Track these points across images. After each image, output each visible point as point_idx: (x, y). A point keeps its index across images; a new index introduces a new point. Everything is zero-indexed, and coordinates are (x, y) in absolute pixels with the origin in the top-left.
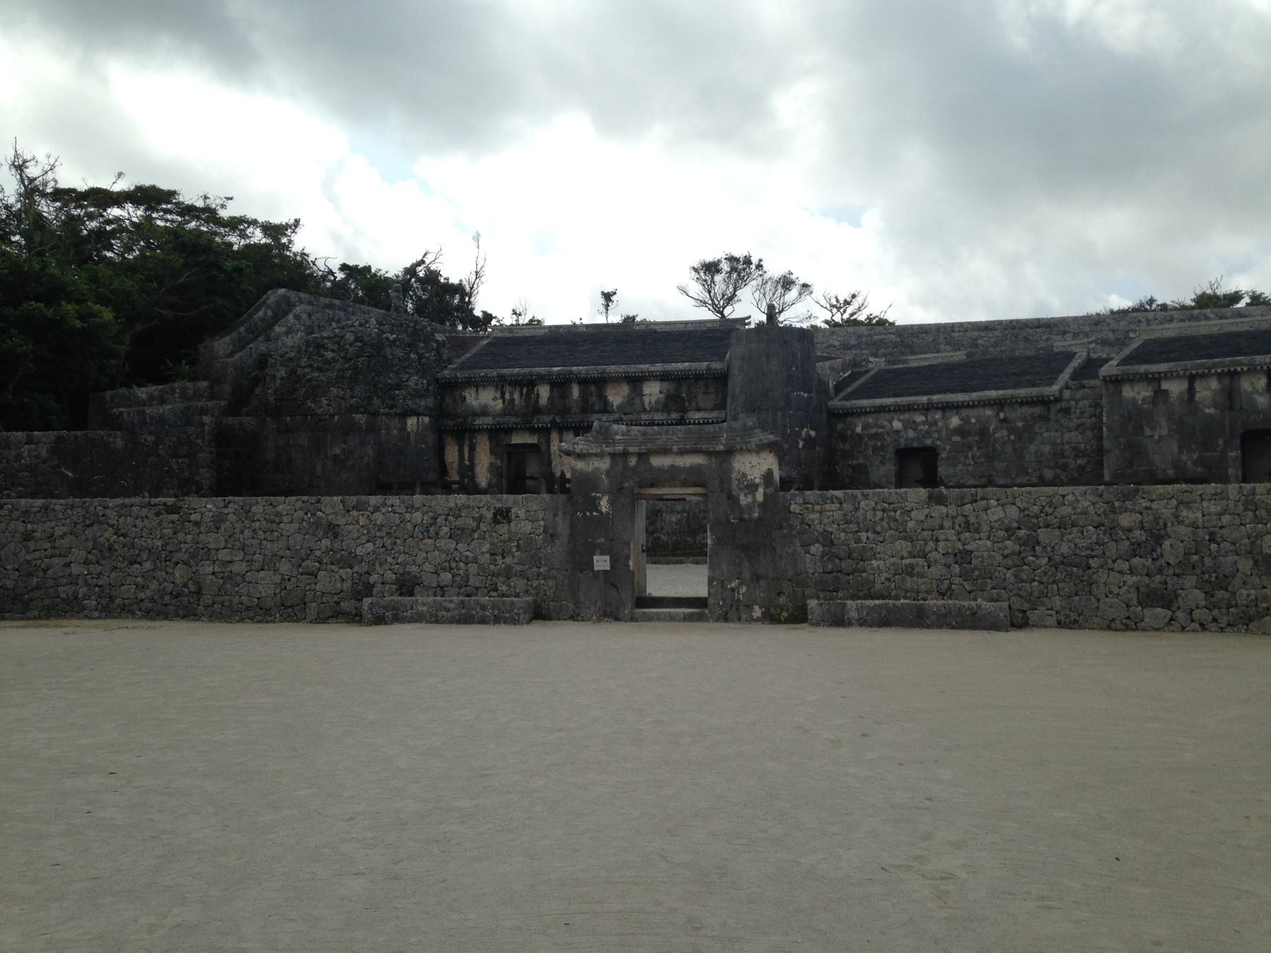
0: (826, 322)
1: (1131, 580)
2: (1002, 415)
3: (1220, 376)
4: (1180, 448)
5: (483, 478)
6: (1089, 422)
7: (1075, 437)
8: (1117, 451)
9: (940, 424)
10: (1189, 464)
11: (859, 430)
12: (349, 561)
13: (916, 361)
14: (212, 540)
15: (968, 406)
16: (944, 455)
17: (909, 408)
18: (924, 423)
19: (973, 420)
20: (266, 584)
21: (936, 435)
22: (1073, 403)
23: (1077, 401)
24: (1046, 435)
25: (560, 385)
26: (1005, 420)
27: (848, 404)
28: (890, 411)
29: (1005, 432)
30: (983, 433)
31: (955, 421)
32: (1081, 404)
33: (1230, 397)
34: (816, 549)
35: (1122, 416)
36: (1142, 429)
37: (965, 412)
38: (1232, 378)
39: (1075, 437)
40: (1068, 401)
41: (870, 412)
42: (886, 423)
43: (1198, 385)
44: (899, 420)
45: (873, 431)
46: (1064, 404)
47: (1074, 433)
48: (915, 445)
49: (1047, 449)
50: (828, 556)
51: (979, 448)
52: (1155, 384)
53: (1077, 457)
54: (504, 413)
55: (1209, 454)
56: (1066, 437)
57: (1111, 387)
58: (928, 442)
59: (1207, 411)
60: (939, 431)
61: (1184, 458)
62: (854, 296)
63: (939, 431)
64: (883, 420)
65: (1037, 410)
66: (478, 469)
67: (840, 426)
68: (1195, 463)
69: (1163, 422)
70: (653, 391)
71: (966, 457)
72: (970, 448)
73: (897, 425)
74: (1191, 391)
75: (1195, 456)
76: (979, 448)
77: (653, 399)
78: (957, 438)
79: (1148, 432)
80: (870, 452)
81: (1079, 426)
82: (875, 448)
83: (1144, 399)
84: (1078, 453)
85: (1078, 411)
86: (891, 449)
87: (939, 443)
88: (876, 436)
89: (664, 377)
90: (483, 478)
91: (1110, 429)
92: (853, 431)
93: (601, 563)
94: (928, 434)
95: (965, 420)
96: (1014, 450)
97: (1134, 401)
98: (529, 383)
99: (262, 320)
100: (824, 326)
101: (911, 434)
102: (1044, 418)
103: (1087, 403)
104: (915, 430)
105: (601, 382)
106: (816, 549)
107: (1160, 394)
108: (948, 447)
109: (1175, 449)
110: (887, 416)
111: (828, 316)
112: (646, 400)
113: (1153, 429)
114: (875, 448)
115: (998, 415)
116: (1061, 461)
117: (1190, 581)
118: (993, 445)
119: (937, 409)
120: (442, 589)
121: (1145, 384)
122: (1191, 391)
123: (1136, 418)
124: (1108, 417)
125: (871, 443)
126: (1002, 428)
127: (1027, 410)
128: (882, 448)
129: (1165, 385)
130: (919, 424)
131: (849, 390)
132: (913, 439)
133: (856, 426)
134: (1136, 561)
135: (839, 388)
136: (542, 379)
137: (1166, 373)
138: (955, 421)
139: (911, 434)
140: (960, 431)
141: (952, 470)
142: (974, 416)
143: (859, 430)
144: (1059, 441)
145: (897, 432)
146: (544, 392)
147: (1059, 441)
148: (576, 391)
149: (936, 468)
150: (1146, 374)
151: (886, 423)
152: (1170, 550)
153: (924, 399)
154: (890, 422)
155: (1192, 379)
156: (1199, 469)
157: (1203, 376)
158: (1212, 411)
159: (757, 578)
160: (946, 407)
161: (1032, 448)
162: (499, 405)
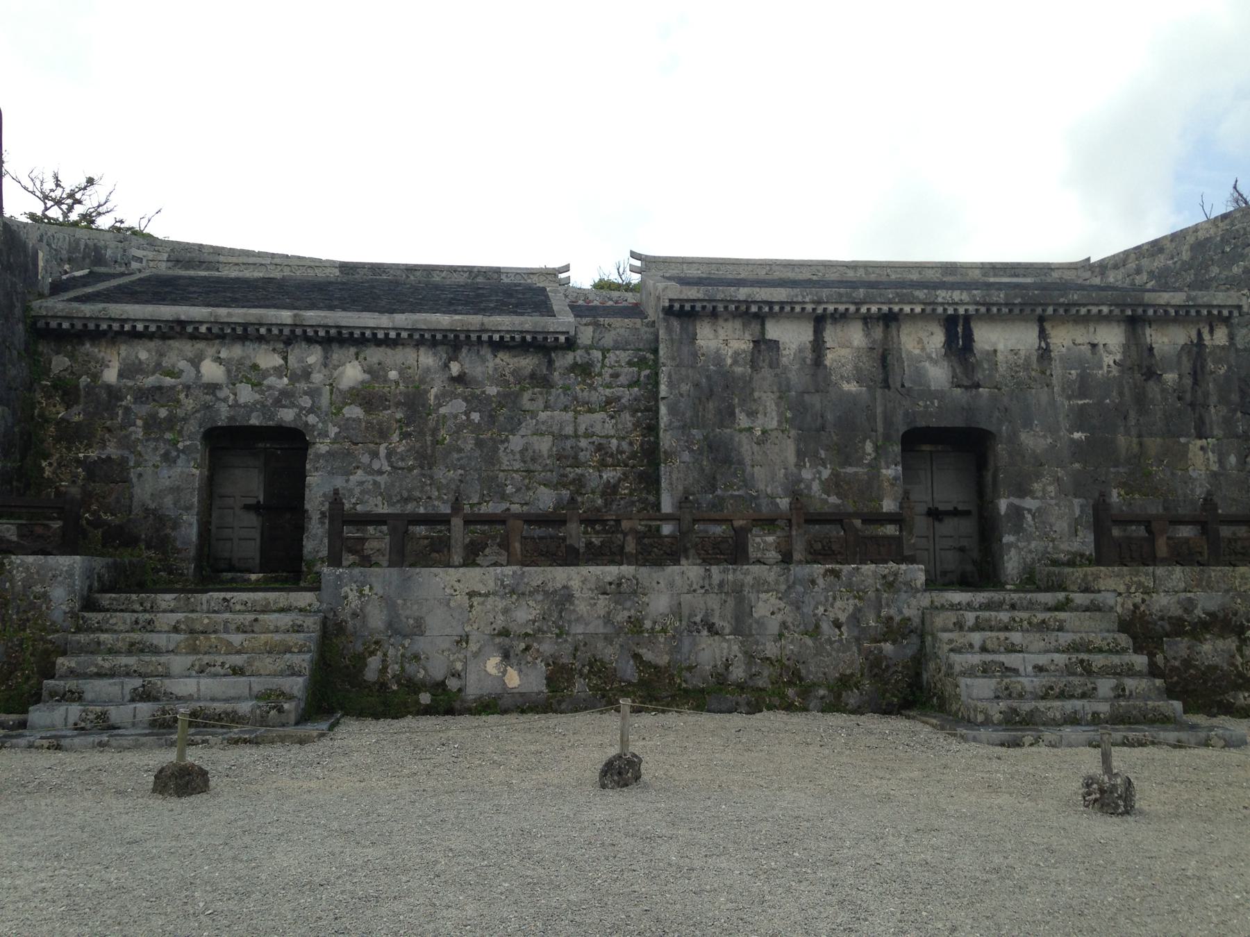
0: (32, 216)
2: (455, 368)
3: (867, 320)
4: (800, 454)
6: (627, 395)
7: (599, 422)
8: (686, 456)
9: (317, 378)
10: (816, 486)
15: (378, 343)
16: (322, 447)
18: (279, 372)
19: (393, 375)
21: (306, 402)
22: (597, 354)
23: (605, 351)
24: (543, 416)
26: (460, 379)
27: (88, 309)
28: (195, 337)
29: (459, 406)
30: (415, 403)
31: (352, 373)
32: (611, 357)
33: (884, 360)
35: (697, 385)
36: (733, 414)
37: (375, 355)
38: (887, 326)
39: (599, 422)
40: (588, 349)
41: (150, 336)
42: (182, 364)
43: (831, 335)
44: (218, 360)
45: (150, 381)
46: (578, 356)
47: (600, 416)
48: (254, 421)
49: (544, 445)
51: (406, 435)
52: (755, 327)
53: (603, 465)
55: (850, 470)
56: (585, 420)
57: (676, 324)
58: (287, 416)
59: (845, 387)
60: (314, 393)
61: (807, 474)
62: (91, 181)
63: (314, 393)
64: (178, 354)
65: (527, 363)
67: (60, 363)
68: (827, 487)
69: (769, 400)
71: (375, 455)
72: (384, 434)
73: (211, 371)
74: (818, 346)
75: (826, 473)
76: (406, 435)
78: (353, 412)
79: (743, 420)
80: (138, 432)
81: (609, 402)
82: (152, 423)
83: (737, 353)
84: (605, 457)
85: (607, 372)
86: (193, 427)
87: (312, 419)
91: (673, 410)
92: (96, 376)
94: (285, 397)
95: (376, 373)
96: (479, 443)
97: (718, 359)
100: (24, 219)
101: (246, 394)
102: (541, 381)
103: (624, 356)
104: (256, 385)
107: (764, 347)
108: (333, 431)
109: (792, 458)
110: (189, 348)
111: (38, 208)
113: (752, 414)
114: (152, 423)
115: (446, 366)
116: (572, 473)
118: (435, 431)
119: (310, 341)
121: (738, 324)
122: (818, 346)
123: (721, 393)
124: (671, 385)
125: (144, 410)
126: (454, 396)
127: (507, 362)
128: (171, 422)
129: (773, 331)
130: (265, 374)
131: (89, 290)
132: (250, 408)
133: (104, 365)
135: (58, 288)
137: (782, 304)
138: (352, 373)
139: (246, 394)
140: (366, 397)
142: (396, 362)
143: (110, 375)
144: (569, 430)
145: (213, 388)
147: (569, 430)
149: (303, 476)
150: (748, 303)
151: (182, 364)
153: (286, 316)
154: (196, 362)
155: (820, 321)
156: (833, 499)
157: (841, 318)
158: (851, 387)
161: (516, 443)
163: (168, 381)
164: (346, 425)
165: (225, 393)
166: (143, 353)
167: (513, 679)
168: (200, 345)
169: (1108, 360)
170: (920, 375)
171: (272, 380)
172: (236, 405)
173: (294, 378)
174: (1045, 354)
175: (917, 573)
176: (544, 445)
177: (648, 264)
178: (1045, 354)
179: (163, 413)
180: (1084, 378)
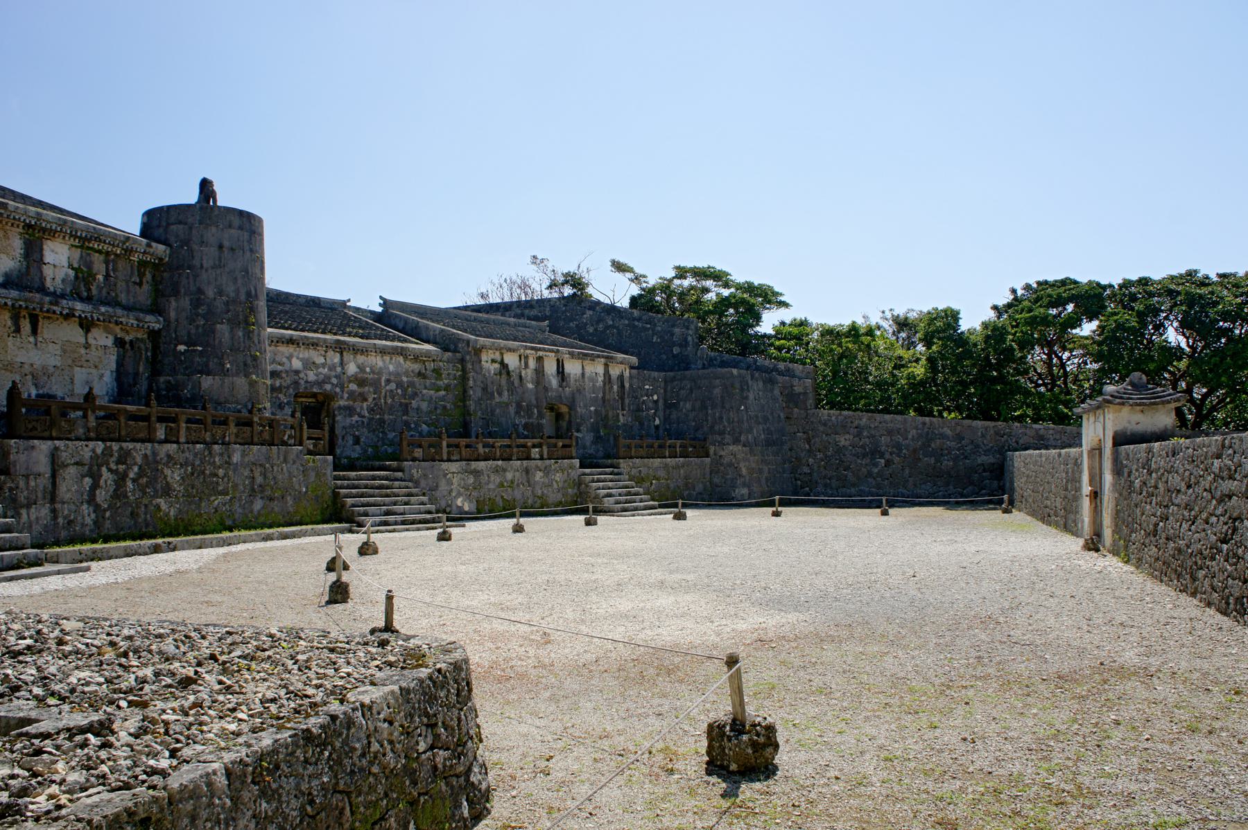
17: (315, 344)
18: (323, 365)
37: (361, 359)
42: (284, 360)
58: (328, 387)
71: (362, 408)
73: (296, 364)
77: (60, 275)
78: (353, 387)
87: (338, 390)
94: (327, 379)
95: (361, 368)
101: (311, 376)
112: (48, 271)
138: (352, 369)
141: (348, 420)
145: (297, 372)
151: (284, 360)
154: (290, 358)
163: (280, 368)
164: (351, 393)
165: (302, 375)
167: (466, 508)
168: (291, 349)
170: (550, 382)
171: (321, 370)
172: (307, 382)
173: (330, 369)
174: (583, 374)
175: (577, 462)
176: (424, 406)
177: (386, 303)
178: (583, 374)
179: (278, 384)
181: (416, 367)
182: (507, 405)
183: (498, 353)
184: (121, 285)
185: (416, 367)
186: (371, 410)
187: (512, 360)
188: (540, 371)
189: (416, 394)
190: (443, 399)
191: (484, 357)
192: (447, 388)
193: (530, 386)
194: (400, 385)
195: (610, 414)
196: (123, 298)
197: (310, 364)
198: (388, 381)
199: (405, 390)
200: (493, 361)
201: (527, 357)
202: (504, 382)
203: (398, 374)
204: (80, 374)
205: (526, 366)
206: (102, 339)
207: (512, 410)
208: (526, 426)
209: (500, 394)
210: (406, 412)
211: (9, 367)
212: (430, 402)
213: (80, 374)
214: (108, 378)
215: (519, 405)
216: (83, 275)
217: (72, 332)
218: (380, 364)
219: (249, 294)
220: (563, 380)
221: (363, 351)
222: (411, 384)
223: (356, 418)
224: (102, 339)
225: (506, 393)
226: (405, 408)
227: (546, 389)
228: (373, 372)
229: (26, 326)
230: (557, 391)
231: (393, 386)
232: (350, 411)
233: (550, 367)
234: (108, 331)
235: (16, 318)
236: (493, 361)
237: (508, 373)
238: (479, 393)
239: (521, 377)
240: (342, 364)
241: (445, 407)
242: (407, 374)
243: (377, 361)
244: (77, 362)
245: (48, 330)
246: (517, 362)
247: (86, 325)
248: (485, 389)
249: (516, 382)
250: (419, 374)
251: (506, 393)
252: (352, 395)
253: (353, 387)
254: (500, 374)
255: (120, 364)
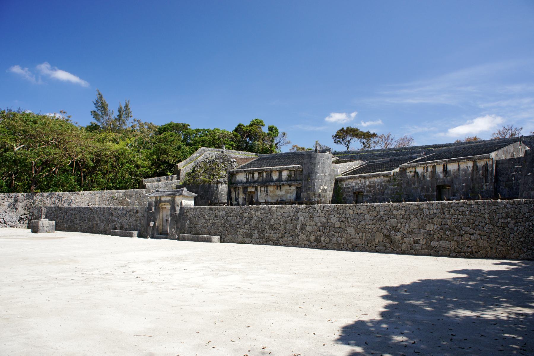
1: (245, 231)
5: (241, 201)
11: (344, 186)
12: (113, 221)
13: (376, 161)
14: (96, 216)
20: (102, 226)
25: (260, 173)
34: (188, 222)
37: (370, 179)
49: (389, 192)
50: (190, 223)
54: (247, 182)
58: (361, 189)
66: (239, 199)
70: (285, 174)
73: (354, 184)
78: (368, 188)
88: (349, 188)
89: (287, 169)
90: (241, 201)
93: (152, 224)
95: (370, 182)
98: (253, 173)
99: (196, 157)
101: (357, 187)
105: (271, 171)
106: (188, 222)
112: (283, 177)
117: (256, 231)
120: (126, 229)
134: (246, 226)
136: (255, 171)
138: (367, 183)
146: (256, 175)
148: (265, 174)
152: (253, 223)
158: (428, 179)
159: (177, 228)
160: (365, 178)
162: (245, 180)
164: (367, 190)
166: (347, 182)
169: (470, 169)
170: (439, 176)
176: (389, 192)
178: (459, 169)
180: (465, 173)
181: (387, 179)
182: (417, 188)
183: (414, 168)
184: (298, 176)
185: (387, 179)
186: (373, 195)
187: (420, 170)
188: (434, 172)
189: (386, 188)
190: (396, 189)
191: (408, 171)
192: (398, 185)
193: (428, 179)
194: (382, 186)
195: (477, 186)
196: (298, 178)
197: (357, 184)
198: (378, 185)
199: (383, 188)
200: (411, 172)
201: (427, 167)
202: (416, 179)
203: (381, 183)
204: (288, 195)
205: (427, 171)
206: (293, 188)
207: (419, 190)
208: (425, 196)
209: (414, 184)
210: (383, 195)
211: (276, 195)
212: (391, 190)
213: (288, 195)
214: (294, 195)
215: (423, 188)
216: (289, 176)
217: (287, 188)
218: (376, 180)
219: (309, 173)
220: (446, 174)
221: (372, 177)
222: (385, 185)
223: (368, 198)
224: (293, 188)
225: (417, 184)
226: (383, 193)
227: (437, 179)
228: (373, 183)
229: (279, 188)
230: (442, 179)
231: (379, 186)
232: (367, 196)
233: (439, 169)
234: (294, 186)
235: (277, 187)
236: (411, 172)
237: (418, 176)
238: (405, 185)
239: (424, 176)
240: (365, 182)
241: (397, 192)
242: (384, 182)
243: (375, 179)
244: (288, 193)
245: (283, 188)
246: (423, 170)
247: (290, 186)
248: (408, 183)
249: (422, 179)
250: (388, 181)
251: (417, 184)
252: (368, 191)
253: (368, 188)
254: (414, 176)
255: (297, 192)
